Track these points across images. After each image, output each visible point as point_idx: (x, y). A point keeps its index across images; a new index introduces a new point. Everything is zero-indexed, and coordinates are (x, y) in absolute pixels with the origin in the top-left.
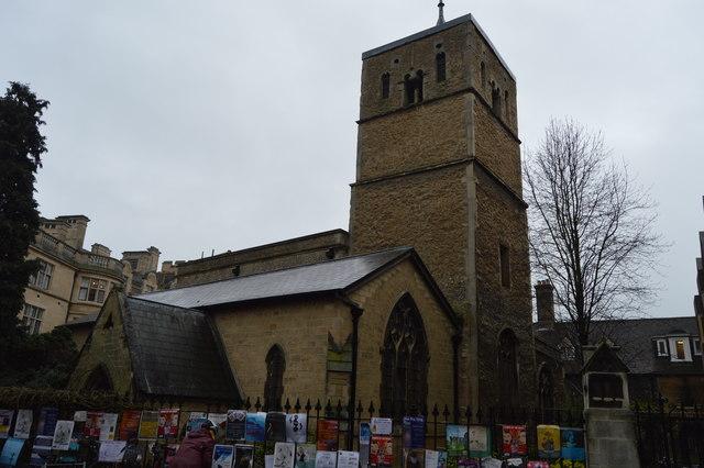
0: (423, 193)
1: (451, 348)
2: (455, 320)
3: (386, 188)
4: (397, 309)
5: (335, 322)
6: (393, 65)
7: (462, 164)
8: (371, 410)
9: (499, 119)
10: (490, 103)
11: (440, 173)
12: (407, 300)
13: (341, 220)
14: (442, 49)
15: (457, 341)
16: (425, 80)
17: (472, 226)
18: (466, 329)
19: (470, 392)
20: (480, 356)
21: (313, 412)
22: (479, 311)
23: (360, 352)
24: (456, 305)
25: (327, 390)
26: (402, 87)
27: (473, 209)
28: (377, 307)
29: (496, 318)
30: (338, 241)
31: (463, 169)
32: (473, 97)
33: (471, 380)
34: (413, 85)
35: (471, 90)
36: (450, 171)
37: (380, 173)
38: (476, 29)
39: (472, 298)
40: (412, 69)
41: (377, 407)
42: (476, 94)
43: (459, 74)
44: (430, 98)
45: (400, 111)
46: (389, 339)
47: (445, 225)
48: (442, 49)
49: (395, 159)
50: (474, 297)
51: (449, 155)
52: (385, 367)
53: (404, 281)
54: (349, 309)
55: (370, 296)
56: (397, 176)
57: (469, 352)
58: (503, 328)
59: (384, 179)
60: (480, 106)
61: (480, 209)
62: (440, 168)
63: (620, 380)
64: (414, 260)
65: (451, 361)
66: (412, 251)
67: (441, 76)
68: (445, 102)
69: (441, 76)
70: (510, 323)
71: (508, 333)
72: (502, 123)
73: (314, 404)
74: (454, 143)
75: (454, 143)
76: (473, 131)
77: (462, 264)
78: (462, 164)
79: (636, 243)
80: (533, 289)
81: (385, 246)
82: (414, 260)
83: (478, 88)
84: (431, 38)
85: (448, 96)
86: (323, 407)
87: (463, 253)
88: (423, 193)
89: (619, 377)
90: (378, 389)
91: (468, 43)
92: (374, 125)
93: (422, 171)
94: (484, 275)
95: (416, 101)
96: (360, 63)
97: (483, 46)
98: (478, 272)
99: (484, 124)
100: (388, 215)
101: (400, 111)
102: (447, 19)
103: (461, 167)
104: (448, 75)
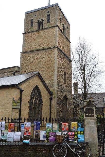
0: (42, 56)
2: (51, 93)
3: (31, 54)
4: (34, 90)
5: (15, 94)
6: (34, 16)
7: (54, 48)
8: (25, 120)
9: (65, 35)
10: (62, 30)
11: (47, 50)
12: (37, 88)
13: (16, 62)
14: (49, 13)
15: (51, 99)
16: (44, 22)
17: (56, 66)
18: (53, 96)
19: (54, 114)
20: (57, 103)
21: (7, 121)
22: (58, 91)
24: (51, 89)
25: (12, 114)
26: (37, 24)
27: (56, 61)
28: (28, 89)
29: (62, 93)
30: (16, 70)
31: (54, 49)
32: (57, 28)
33: (54, 110)
34: (40, 23)
35: (57, 26)
36: (50, 50)
37: (30, 50)
38: (59, 8)
39: (55, 87)
40: (40, 18)
41: (26, 119)
42: (59, 27)
43: (54, 21)
44: (45, 28)
45: (36, 31)
46: (31, 99)
47: (49, 66)
49: (34, 45)
50: (56, 87)
51: (50, 45)
52: (30, 107)
53: (36, 82)
55: (26, 86)
57: (54, 102)
58: (64, 95)
60: (59, 30)
61: (59, 61)
62: (48, 49)
63: (93, 110)
64: (39, 76)
65: (49, 105)
66: (39, 73)
67: (48, 21)
68: (49, 29)
69: (48, 21)
70: (66, 94)
71: (65, 97)
72: (65, 36)
73: (7, 119)
74: (52, 42)
75: (52, 42)
76: (57, 38)
77: (53, 77)
78: (54, 48)
79: (99, 73)
80: (73, 85)
81: (31, 71)
82: (39, 76)
83: (59, 26)
84: (46, 9)
86: (10, 119)
87: (53, 74)
88: (42, 56)
89: (93, 109)
91: (57, 12)
92: (28, 35)
93: (42, 50)
94: (59, 80)
95: (41, 28)
96: (24, 16)
97: (61, 14)
101: (36, 31)
102: (51, 4)
104: (50, 20)
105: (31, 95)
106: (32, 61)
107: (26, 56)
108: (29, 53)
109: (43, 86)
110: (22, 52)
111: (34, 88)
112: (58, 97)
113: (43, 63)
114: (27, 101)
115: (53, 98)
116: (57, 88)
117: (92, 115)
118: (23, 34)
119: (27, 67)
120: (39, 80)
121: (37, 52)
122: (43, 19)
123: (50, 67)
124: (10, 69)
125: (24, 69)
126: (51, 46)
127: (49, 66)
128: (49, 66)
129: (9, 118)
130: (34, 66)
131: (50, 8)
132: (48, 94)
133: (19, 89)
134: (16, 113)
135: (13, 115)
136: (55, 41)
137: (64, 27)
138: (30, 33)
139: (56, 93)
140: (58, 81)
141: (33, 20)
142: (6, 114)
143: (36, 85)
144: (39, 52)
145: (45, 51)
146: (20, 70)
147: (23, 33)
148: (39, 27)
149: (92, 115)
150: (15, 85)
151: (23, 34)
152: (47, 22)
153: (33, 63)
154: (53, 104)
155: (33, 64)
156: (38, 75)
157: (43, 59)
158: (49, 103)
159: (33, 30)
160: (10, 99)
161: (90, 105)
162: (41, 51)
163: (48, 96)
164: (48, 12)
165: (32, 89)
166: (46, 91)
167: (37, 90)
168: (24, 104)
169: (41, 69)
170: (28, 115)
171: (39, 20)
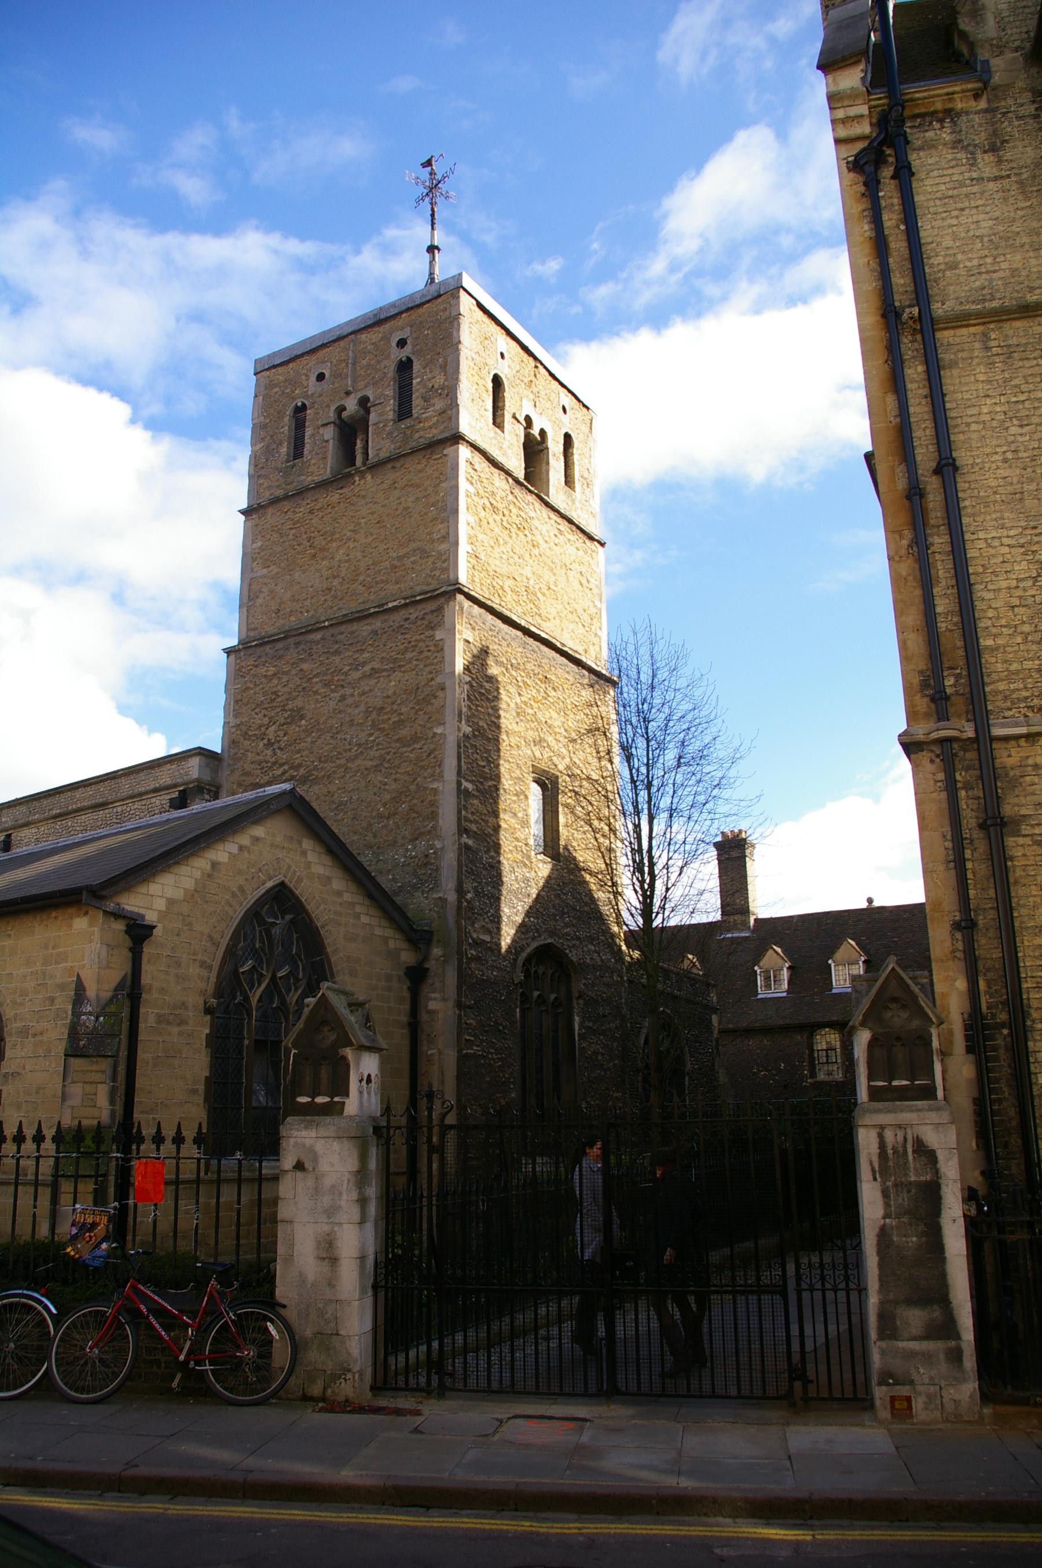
1: (406, 994)
3: (292, 655)
4: (254, 915)
11: (398, 617)
14: (407, 351)
16: (373, 418)
18: (437, 951)
20: (459, 1005)
21: (29, 1146)
23: (148, 1015)
25: (64, 1097)
26: (329, 433)
30: (195, 774)
31: (440, 609)
36: (414, 613)
40: (348, 393)
44: (384, 454)
48: (407, 351)
54: (120, 926)
55: (179, 894)
56: (314, 628)
59: (287, 635)
62: (395, 609)
65: (404, 1019)
67: (404, 410)
69: (404, 410)
74: (424, 554)
77: (434, 816)
85: (415, 451)
86: (49, 1133)
87: (435, 791)
88: (364, 664)
90: (201, 1088)
92: (272, 516)
98: (462, 830)
99: (495, 509)
100: (298, 714)
103: (432, 606)
104: (417, 402)
105: (230, 952)
106: (298, 703)
107: (262, 670)
108: (280, 645)
109: (339, 882)
110: (234, 642)
111: (260, 902)
112: (477, 959)
113: (368, 712)
114: (196, 1001)
115: (431, 964)
116: (460, 891)
117: (336, 1099)
118: (243, 512)
119: (269, 752)
120: (307, 844)
121: (328, 633)
122: (370, 393)
123: (415, 738)
124: (157, 772)
125: (248, 767)
126: (418, 589)
127: (405, 732)
128: (405, 732)
129: (39, 1130)
130: (309, 739)
131: (414, 315)
132: (396, 942)
133: (118, 915)
134: (89, 1088)
135: (69, 1103)
136: (443, 547)
137: (528, 436)
138: (286, 505)
139: (454, 933)
140: (470, 842)
141: (304, 408)
142: (37, 1093)
143: (270, 884)
144: (341, 637)
145: (377, 624)
146: (226, 772)
147: (244, 505)
148: (349, 458)
149: (336, 1099)
150: (85, 894)
151: (243, 512)
152: (391, 416)
153: (302, 717)
154: (429, 1012)
155: (303, 722)
156: (290, 807)
157: (373, 682)
158: (406, 1007)
159: (308, 480)
160: (62, 987)
161: (326, 1029)
162: (355, 626)
163: (393, 955)
164: (402, 343)
165: (241, 912)
166: (375, 921)
167: (288, 917)
168: (160, 1019)
169: (356, 757)
170: (206, 1100)
171: (341, 409)
